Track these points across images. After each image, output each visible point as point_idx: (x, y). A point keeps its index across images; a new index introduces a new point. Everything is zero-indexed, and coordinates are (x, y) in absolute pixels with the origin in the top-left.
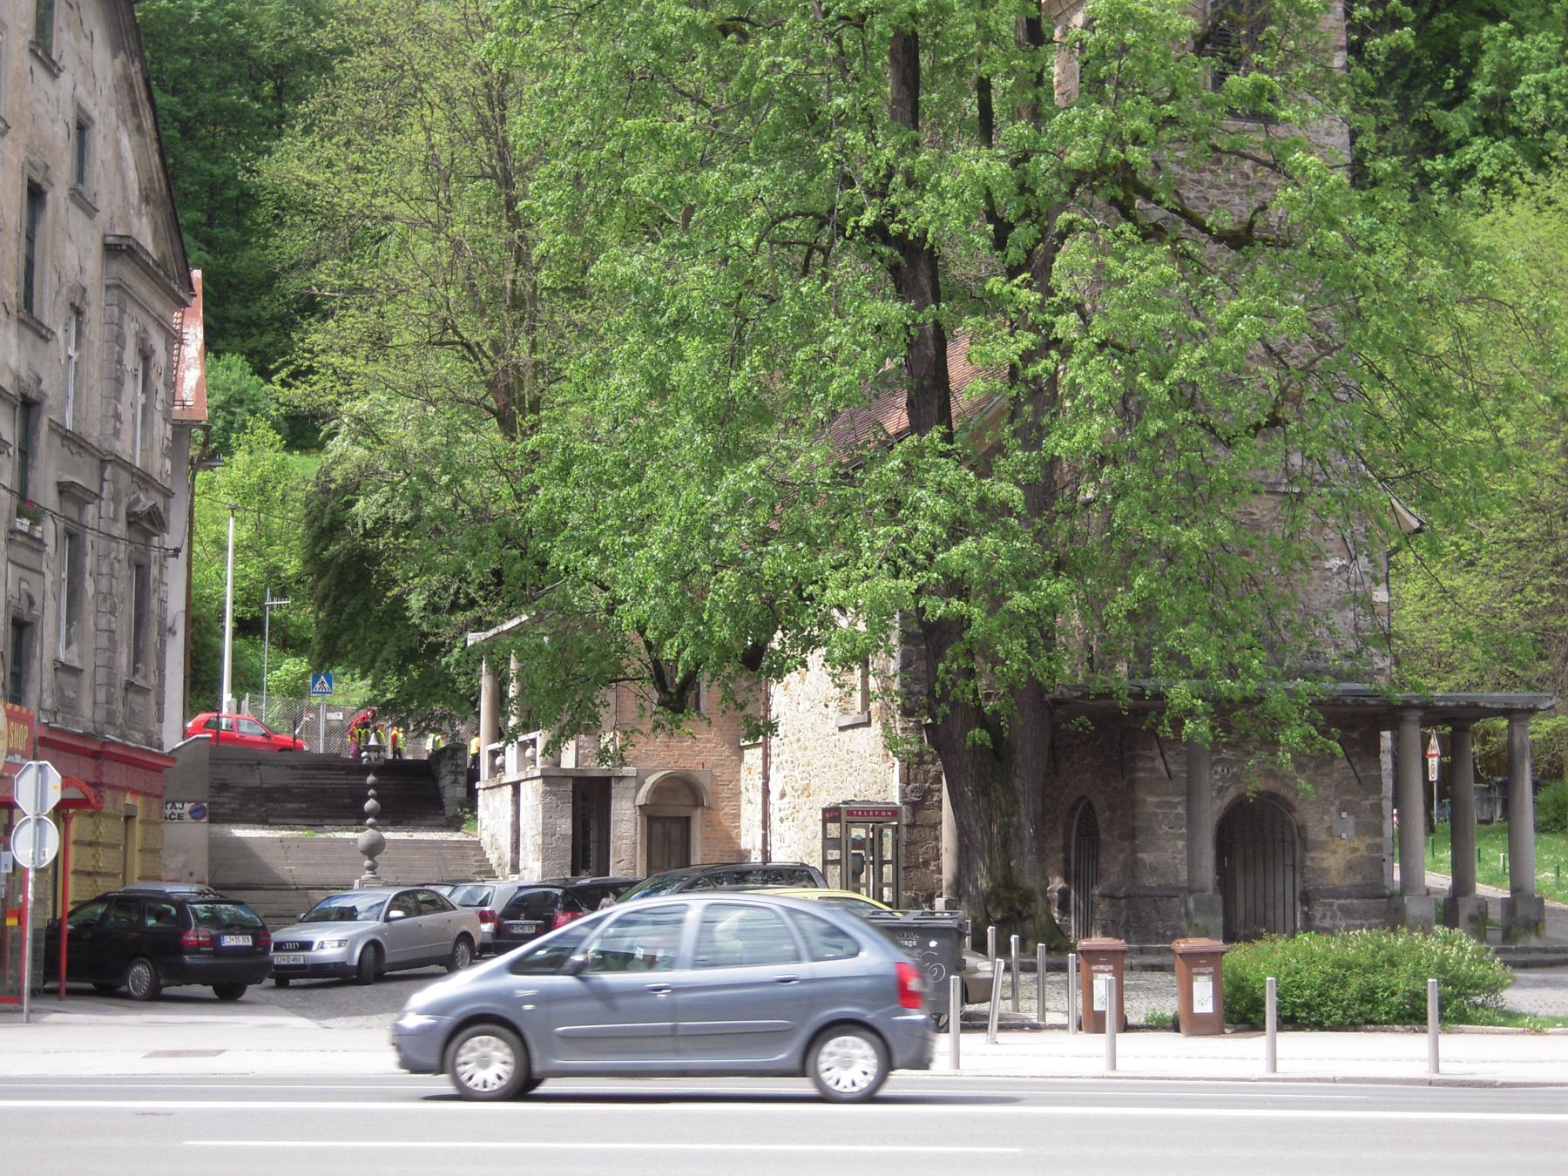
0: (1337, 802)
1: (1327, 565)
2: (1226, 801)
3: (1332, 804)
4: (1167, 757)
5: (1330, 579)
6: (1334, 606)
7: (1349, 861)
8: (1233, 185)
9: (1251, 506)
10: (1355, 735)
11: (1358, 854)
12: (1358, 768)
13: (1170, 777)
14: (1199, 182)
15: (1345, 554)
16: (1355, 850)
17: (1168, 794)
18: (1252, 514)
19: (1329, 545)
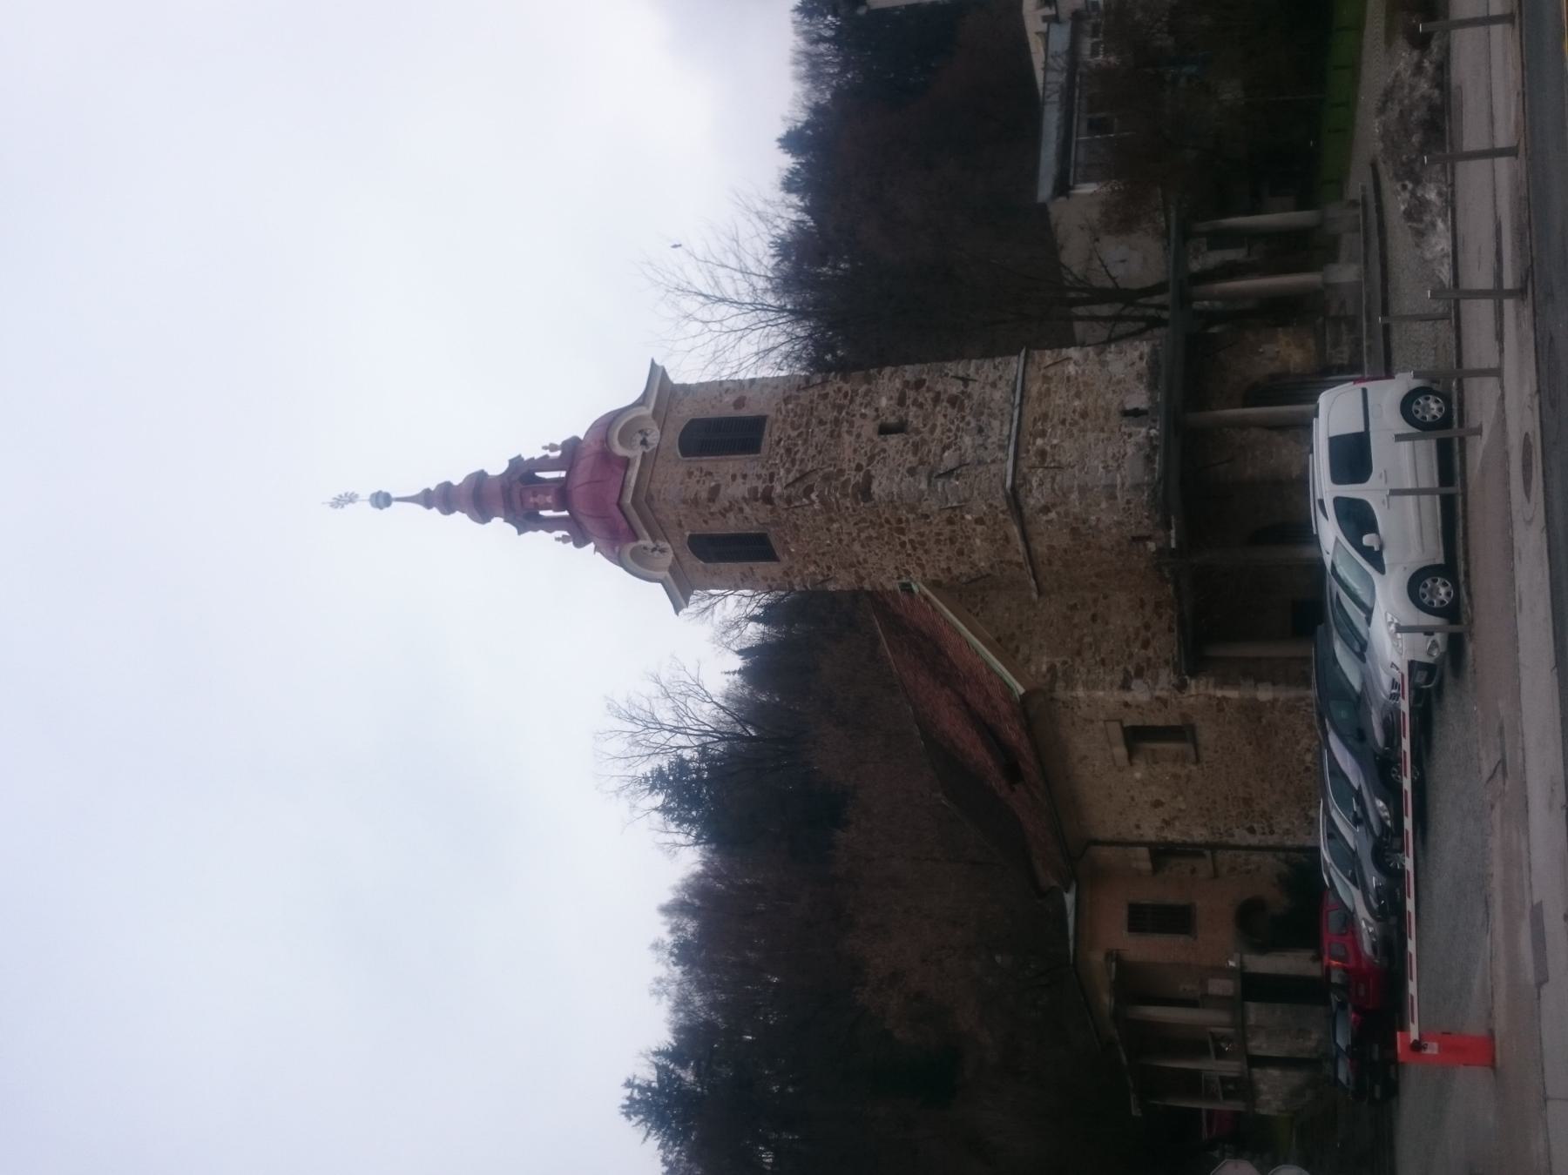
1: (1073, 373)
8: (805, 441)
15: (1066, 362)
18: (1035, 419)
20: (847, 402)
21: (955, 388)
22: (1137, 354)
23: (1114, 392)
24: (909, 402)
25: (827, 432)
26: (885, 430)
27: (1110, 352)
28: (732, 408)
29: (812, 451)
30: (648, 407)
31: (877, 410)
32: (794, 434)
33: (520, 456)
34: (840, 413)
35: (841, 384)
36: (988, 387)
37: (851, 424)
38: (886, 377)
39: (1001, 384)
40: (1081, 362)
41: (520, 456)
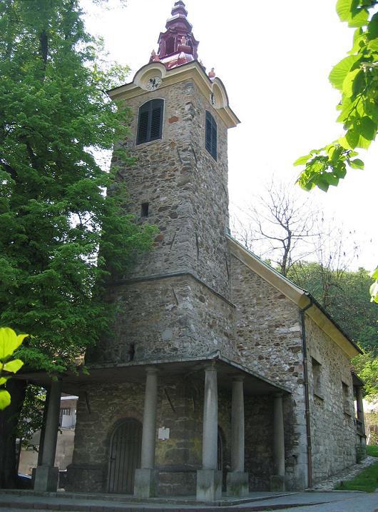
0: (163, 422)
1: (167, 308)
2: (113, 423)
3: (160, 422)
4: (89, 403)
5: (168, 314)
6: (169, 327)
7: (167, 452)
8: (142, 166)
9: (135, 288)
10: (174, 387)
11: (172, 448)
12: (173, 404)
13: (90, 413)
14: (130, 169)
16: (170, 446)
17: (88, 421)
18: (136, 291)
19: (168, 299)
20: (167, 177)
21: (167, 239)
22: (177, 346)
23: (149, 336)
24: (161, 214)
25: (148, 175)
26: (145, 207)
27: (180, 329)
28: (170, 117)
29: (134, 172)
30: (166, 75)
31: (158, 197)
32: (148, 158)
33: (161, 33)
34: (159, 177)
35: (180, 169)
36: (166, 257)
37: (149, 187)
38: (183, 194)
39: (166, 265)
40: (175, 311)
41: (161, 33)
